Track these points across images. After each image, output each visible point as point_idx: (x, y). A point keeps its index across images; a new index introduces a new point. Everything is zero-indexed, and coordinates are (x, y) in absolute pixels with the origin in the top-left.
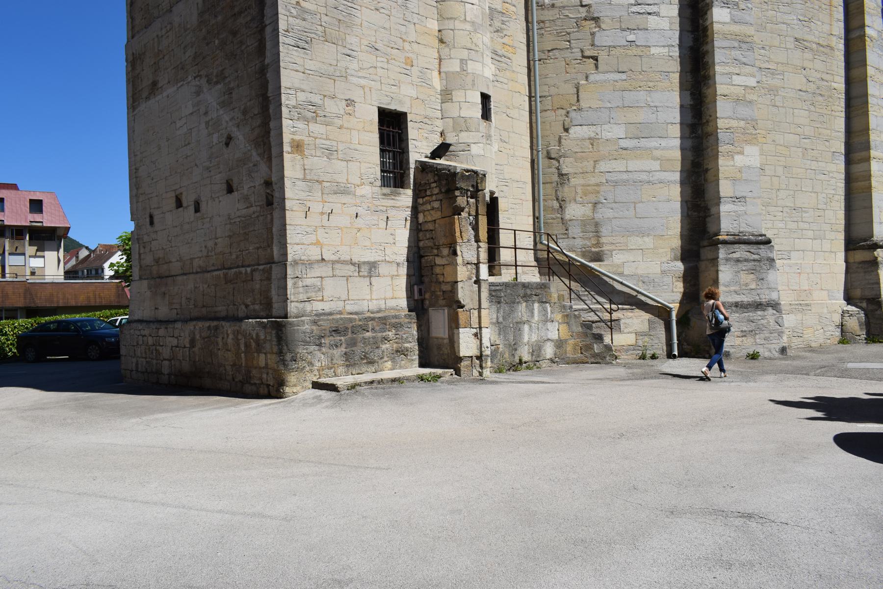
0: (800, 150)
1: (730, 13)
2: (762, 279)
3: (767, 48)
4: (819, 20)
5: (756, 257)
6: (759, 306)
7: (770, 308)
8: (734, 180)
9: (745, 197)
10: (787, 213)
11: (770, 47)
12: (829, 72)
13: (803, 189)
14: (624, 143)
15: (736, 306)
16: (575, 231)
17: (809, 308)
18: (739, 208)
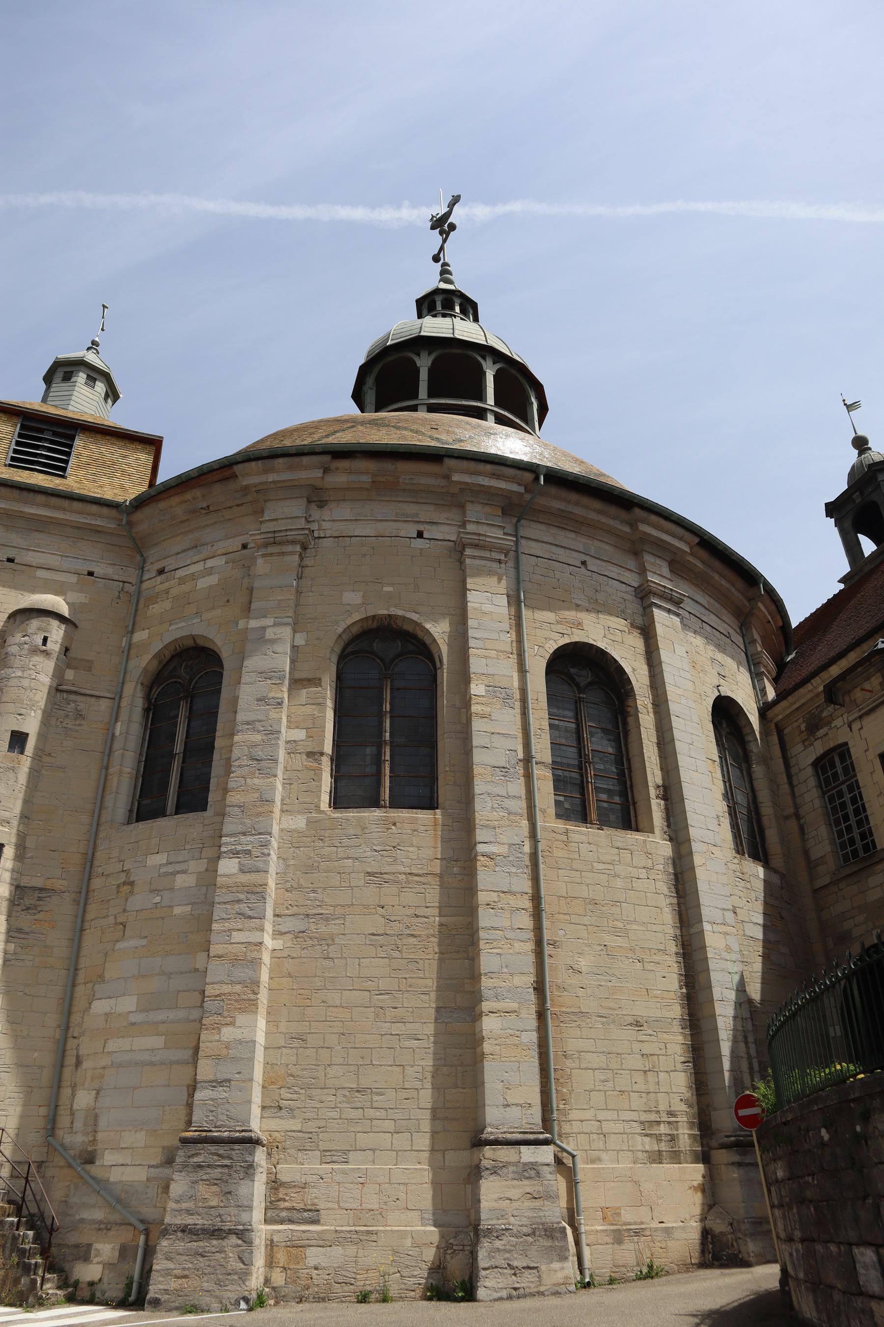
0: (372, 1009)
1: (239, 862)
2: (230, 1193)
3: (320, 890)
4: (412, 845)
5: (227, 1162)
6: (216, 1233)
7: (234, 1236)
8: (218, 1058)
9: (229, 1081)
10: (344, 1096)
11: (325, 889)
12: (428, 905)
13: (374, 1063)
14: (133, 1018)
15: (183, 1231)
16: (78, 1125)
17: (374, 1237)
18: (220, 1093)
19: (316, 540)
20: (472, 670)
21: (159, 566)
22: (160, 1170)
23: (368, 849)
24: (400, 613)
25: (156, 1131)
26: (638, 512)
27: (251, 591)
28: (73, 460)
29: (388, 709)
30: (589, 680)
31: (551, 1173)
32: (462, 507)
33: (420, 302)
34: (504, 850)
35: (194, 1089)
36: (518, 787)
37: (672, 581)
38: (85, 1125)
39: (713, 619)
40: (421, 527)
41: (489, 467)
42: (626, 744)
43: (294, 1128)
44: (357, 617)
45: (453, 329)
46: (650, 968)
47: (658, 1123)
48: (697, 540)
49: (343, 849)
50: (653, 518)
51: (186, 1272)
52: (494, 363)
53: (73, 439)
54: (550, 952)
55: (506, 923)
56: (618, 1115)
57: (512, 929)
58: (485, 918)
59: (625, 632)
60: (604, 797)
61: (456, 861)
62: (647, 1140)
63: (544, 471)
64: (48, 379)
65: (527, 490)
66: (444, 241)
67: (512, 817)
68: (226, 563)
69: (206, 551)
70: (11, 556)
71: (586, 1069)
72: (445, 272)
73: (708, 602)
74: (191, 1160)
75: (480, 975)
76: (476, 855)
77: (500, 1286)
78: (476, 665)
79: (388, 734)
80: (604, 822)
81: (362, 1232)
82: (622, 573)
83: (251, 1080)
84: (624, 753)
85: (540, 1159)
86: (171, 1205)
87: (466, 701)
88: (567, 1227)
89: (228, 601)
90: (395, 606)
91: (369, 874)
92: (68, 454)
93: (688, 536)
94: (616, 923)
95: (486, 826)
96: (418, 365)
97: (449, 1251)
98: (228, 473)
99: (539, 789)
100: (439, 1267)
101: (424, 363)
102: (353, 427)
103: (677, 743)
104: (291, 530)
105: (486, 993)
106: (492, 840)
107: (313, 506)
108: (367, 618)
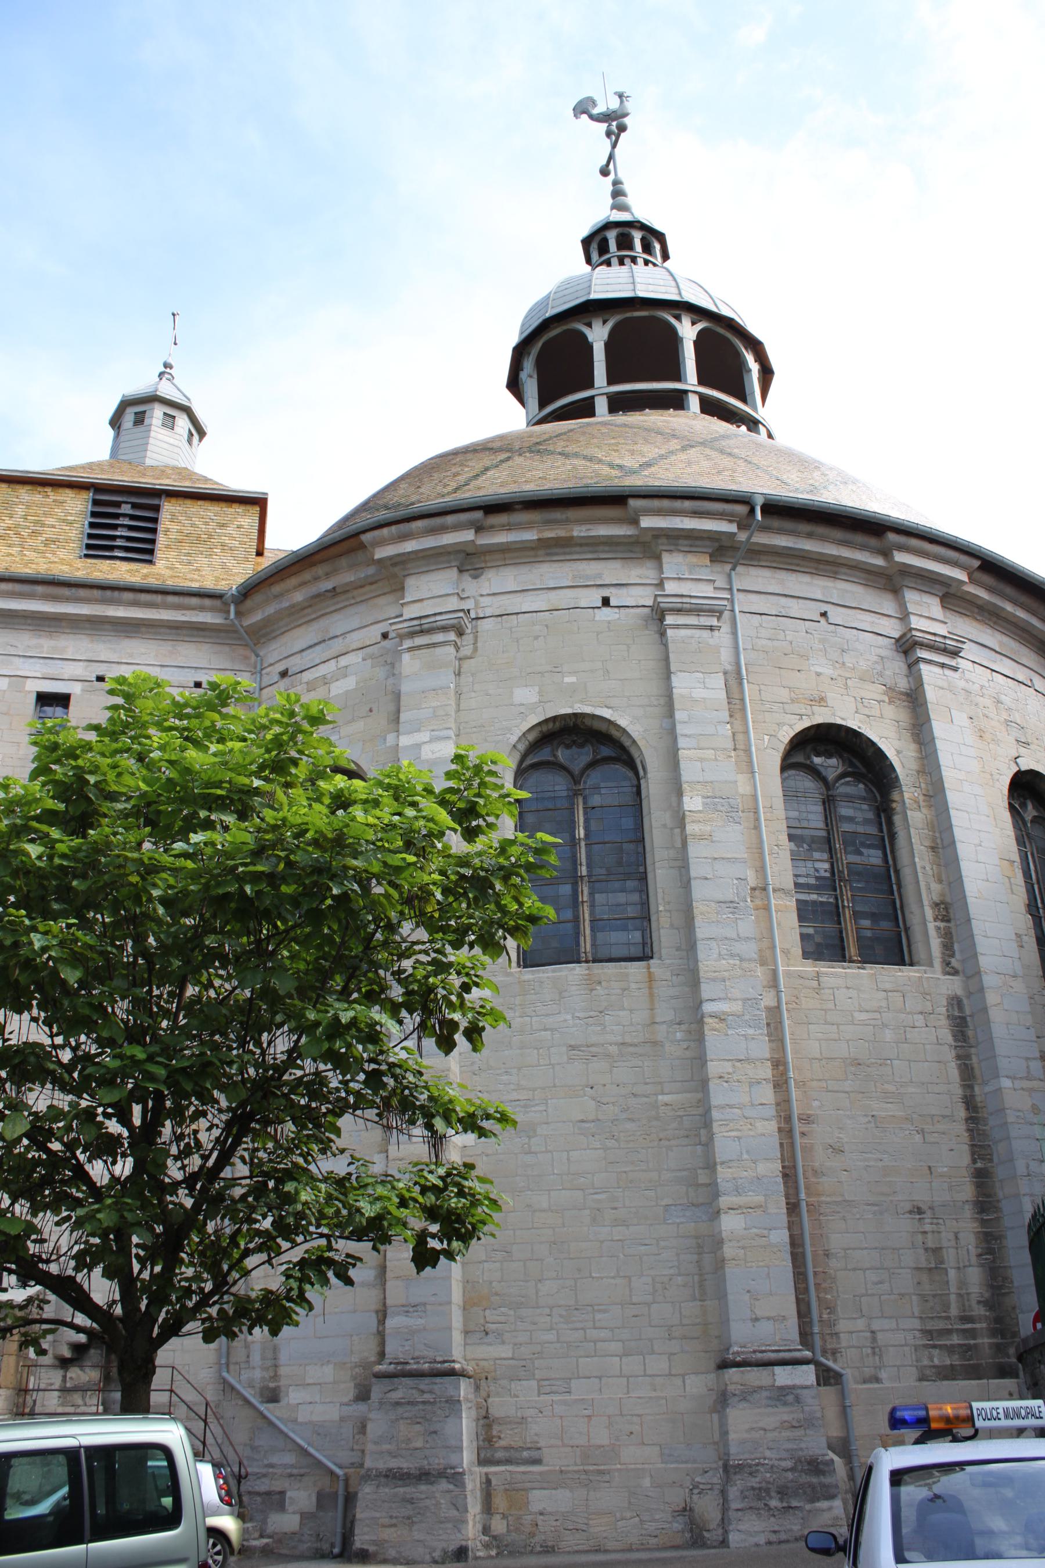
2: (435, 1432)
5: (427, 1397)
6: (424, 1476)
7: (444, 1480)
9: (425, 1304)
10: (561, 1316)
13: (594, 1275)
15: (387, 1476)
17: (607, 1478)
19: (474, 622)
20: (684, 778)
21: (281, 667)
22: (355, 1407)
23: (569, 1017)
24: (588, 710)
25: (345, 1364)
26: (892, 537)
27: (397, 696)
28: (161, 539)
29: (582, 835)
30: (840, 770)
31: (813, 1398)
32: (658, 558)
33: (586, 242)
34: (736, 1007)
35: (385, 1317)
36: (747, 926)
37: (946, 623)
38: (263, 1358)
39: (1006, 666)
40: (606, 592)
41: (687, 504)
42: (893, 852)
43: (504, 1355)
44: (534, 720)
45: (634, 283)
46: (933, 1140)
47: (949, 1332)
48: (976, 563)
49: (538, 1019)
50: (914, 542)
51: (394, 1521)
52: (693, 323)
53: (157, 509)
54: (802, 1130)
55: (745, 1099)
56: (897, 1324)
57: (752, 1105)
58: (718, 1095)
59: (884, 701)
60: (866, 923)
61: (679, 1024)
62: (936, 1352)
63: (759, 501)
64: (115, 422)
65: (740, 527)
66: (614, 146)
67: (745, 965)
68: (364, 660)
69: (337, 646)
70: (101, 674)
71: (854, 1269)
72: (617, 193)
73: (1001, 643)
74: (389, 1395)
75: (715, 1164)
76: (702, 1017)
77: (756, 1529)
78: (689, 771)
79: (584, 868)
80: (867, 957)
81: (593, 1471)
82: (877, 621)
83: (450, 1303)
84: (891, 862)
85: (798, 1382)
86: (370, 1447)
87: (680, 820)
88: (836, 1458)
89: (371, 711)
90: (582, 702)
91: (573, 1048)
92: (154, 531)
93: (964, 559)
94: (886, 1086)
95: (714, 980)
96: (590, 339)
97: (696, 1491)
98: (352, 543)
99: (779, 924)
100: (684, 1509)
101: (598, 335)
102: (508, 459)
103: (959, 846)
104: (440, 614)
105: (723, 1186)
106: (722, 995)
107: (466, 576)
108: (546, 721)
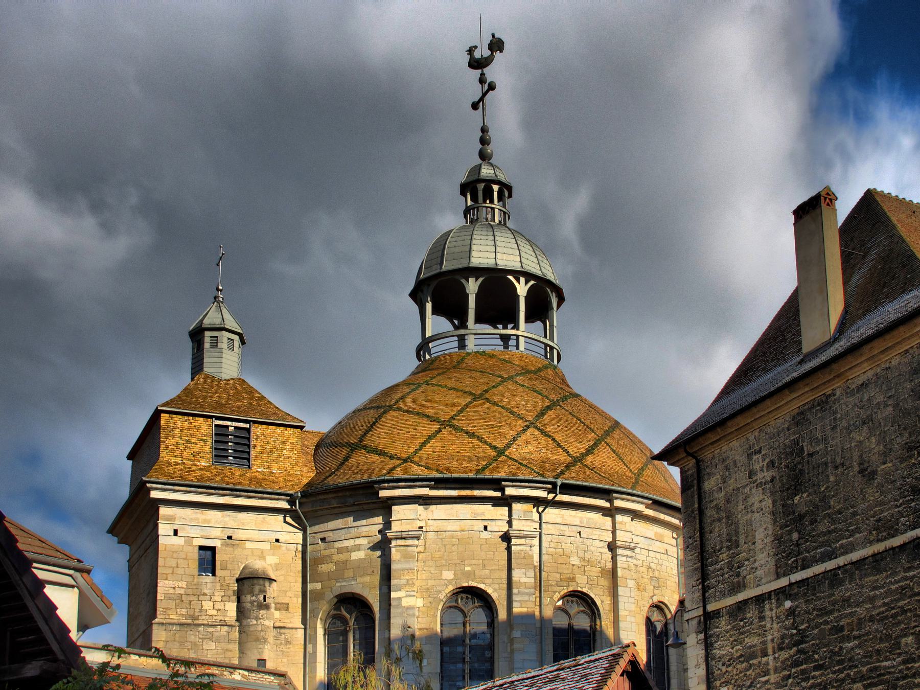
24: (475, 584)
28: (252, 451)
40: (486, 523)
45: (495, 258)
